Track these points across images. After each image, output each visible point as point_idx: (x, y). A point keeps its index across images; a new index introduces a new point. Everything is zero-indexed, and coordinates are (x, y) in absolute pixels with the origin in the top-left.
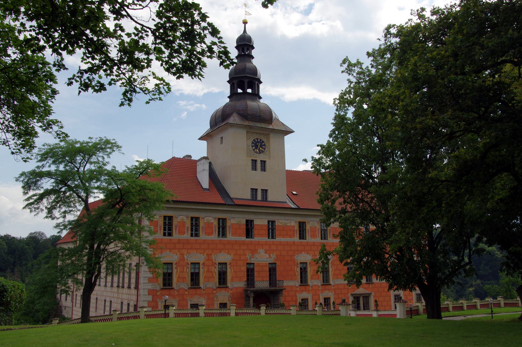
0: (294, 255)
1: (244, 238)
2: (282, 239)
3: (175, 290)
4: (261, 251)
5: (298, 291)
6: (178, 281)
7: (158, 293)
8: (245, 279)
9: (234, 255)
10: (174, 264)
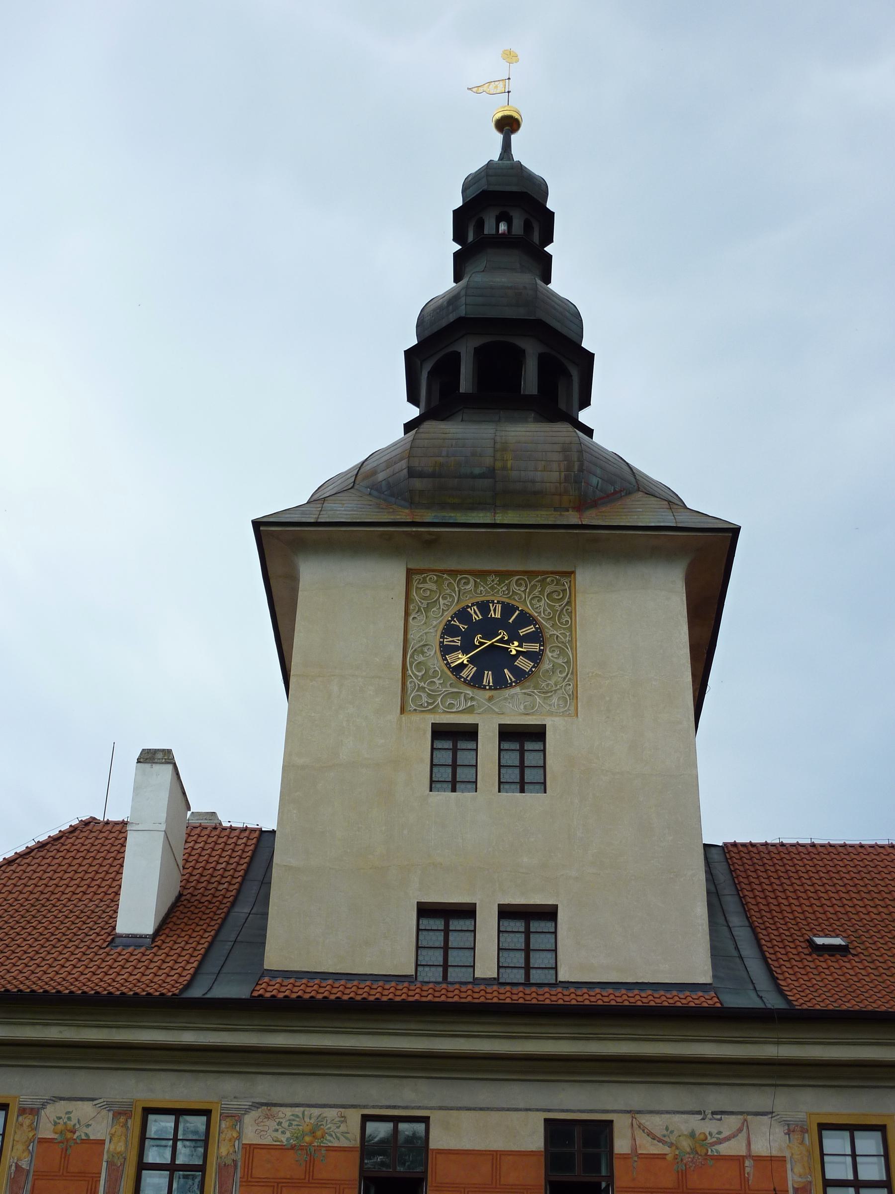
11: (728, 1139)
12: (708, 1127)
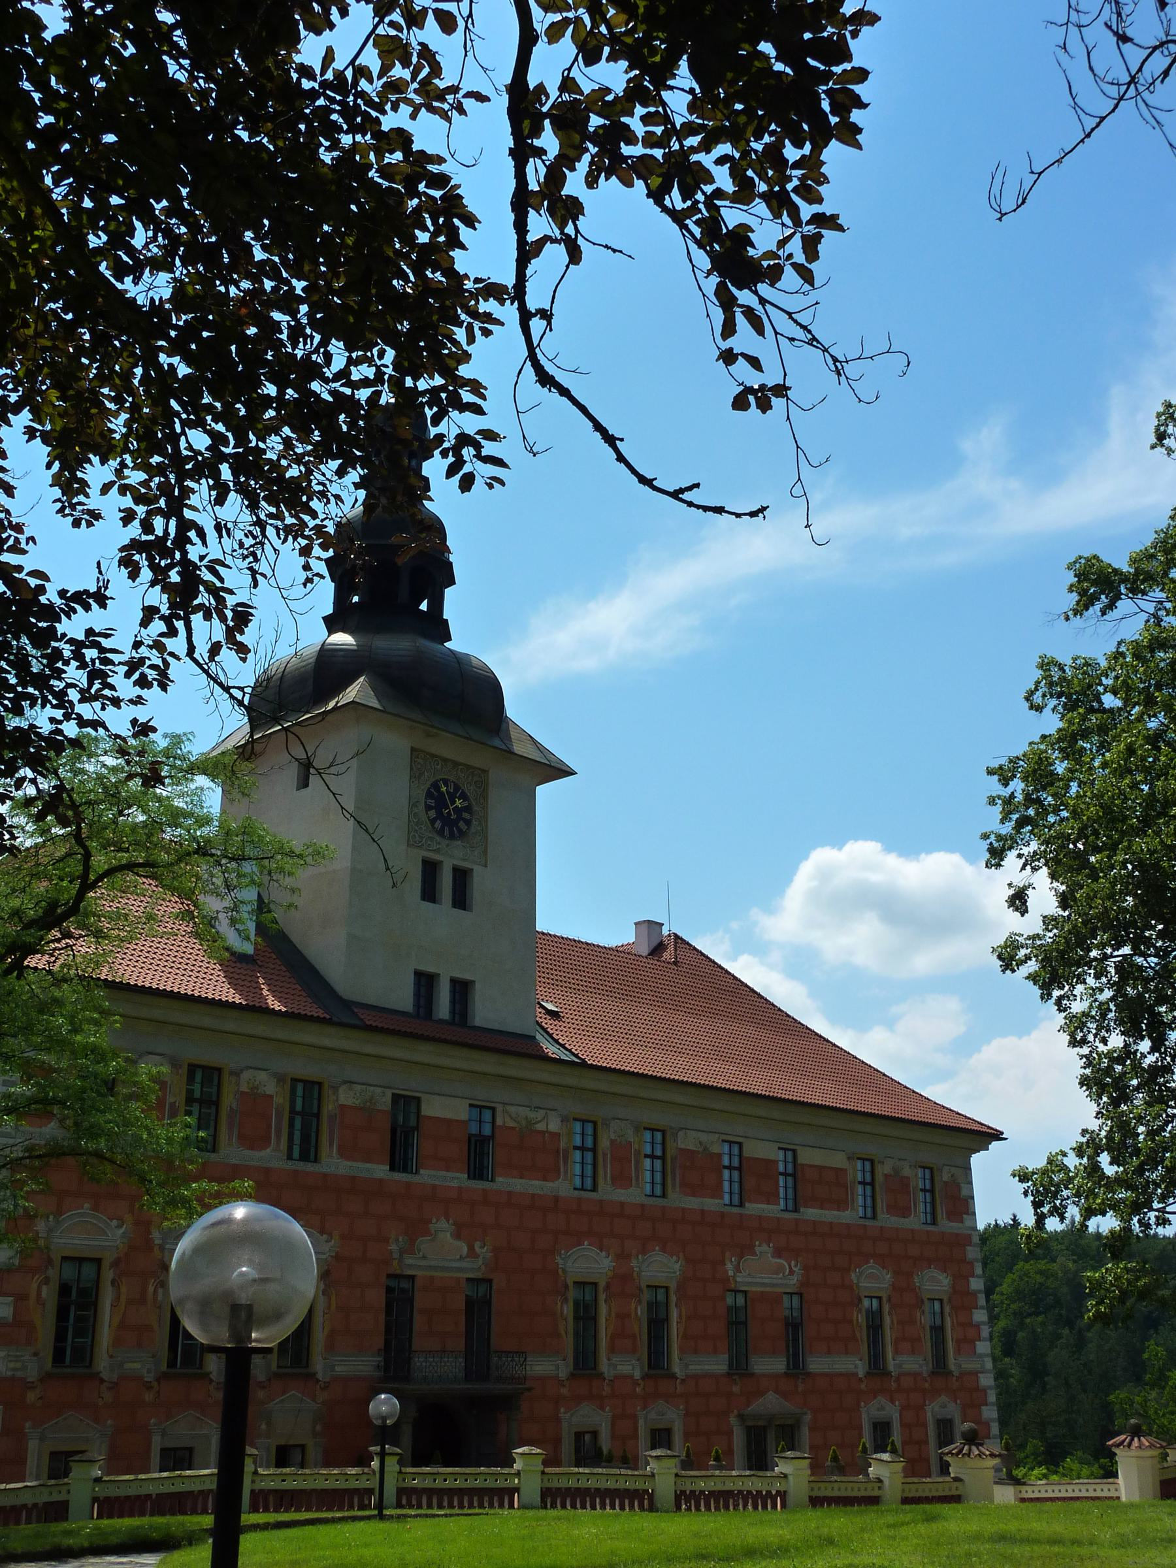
1: (380, 1171)
2: (518, 1185)
3: (102, 1381)
4: (443, 1228)
6: (117, 1342)
7: (31, 1397)
8: (379, 1342)
10: (106, 1265)
11: (540, 1121)
12: (532, 1115)
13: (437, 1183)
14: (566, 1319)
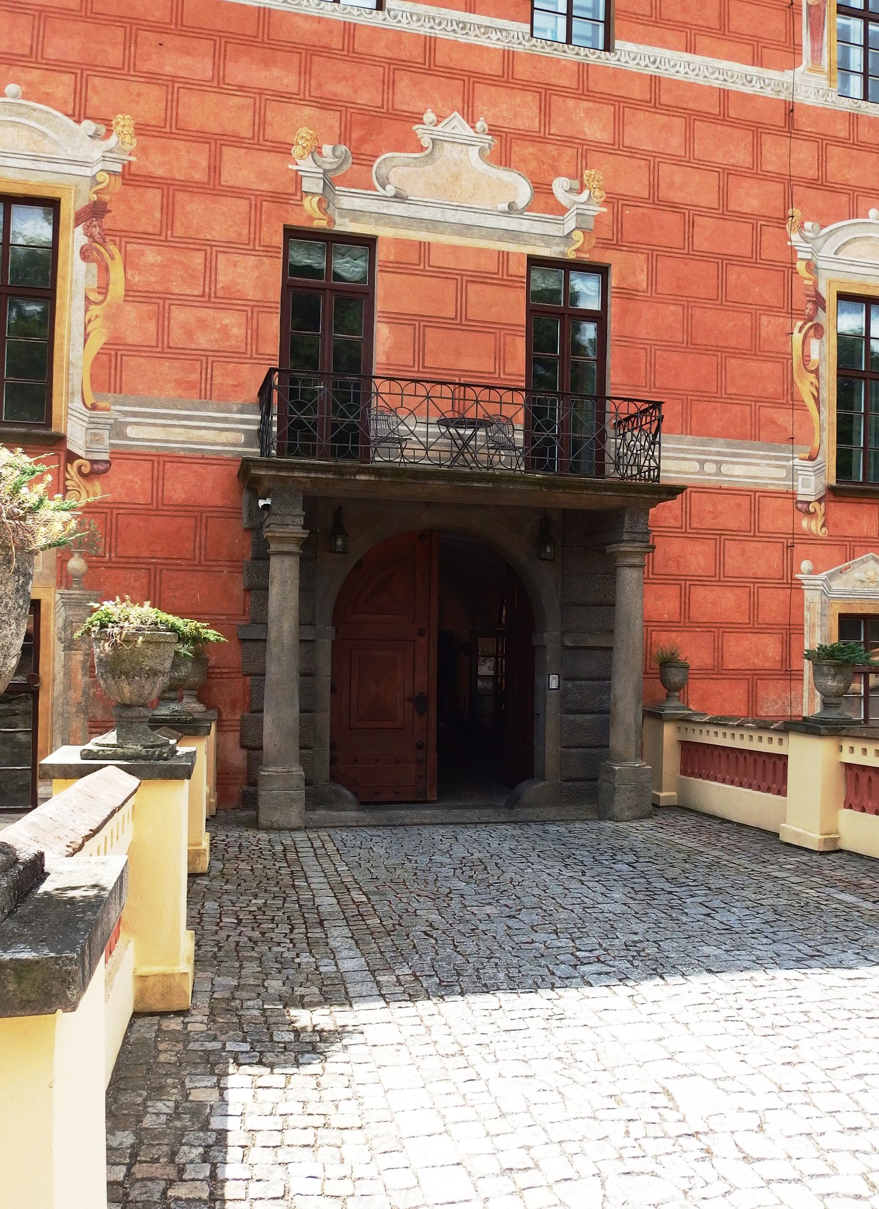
0: (782, 221)
5: (811, 539)
9: (141, 130)
13: (438, 33)
14: (816, 372)
